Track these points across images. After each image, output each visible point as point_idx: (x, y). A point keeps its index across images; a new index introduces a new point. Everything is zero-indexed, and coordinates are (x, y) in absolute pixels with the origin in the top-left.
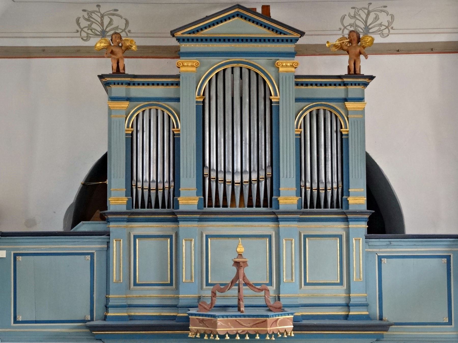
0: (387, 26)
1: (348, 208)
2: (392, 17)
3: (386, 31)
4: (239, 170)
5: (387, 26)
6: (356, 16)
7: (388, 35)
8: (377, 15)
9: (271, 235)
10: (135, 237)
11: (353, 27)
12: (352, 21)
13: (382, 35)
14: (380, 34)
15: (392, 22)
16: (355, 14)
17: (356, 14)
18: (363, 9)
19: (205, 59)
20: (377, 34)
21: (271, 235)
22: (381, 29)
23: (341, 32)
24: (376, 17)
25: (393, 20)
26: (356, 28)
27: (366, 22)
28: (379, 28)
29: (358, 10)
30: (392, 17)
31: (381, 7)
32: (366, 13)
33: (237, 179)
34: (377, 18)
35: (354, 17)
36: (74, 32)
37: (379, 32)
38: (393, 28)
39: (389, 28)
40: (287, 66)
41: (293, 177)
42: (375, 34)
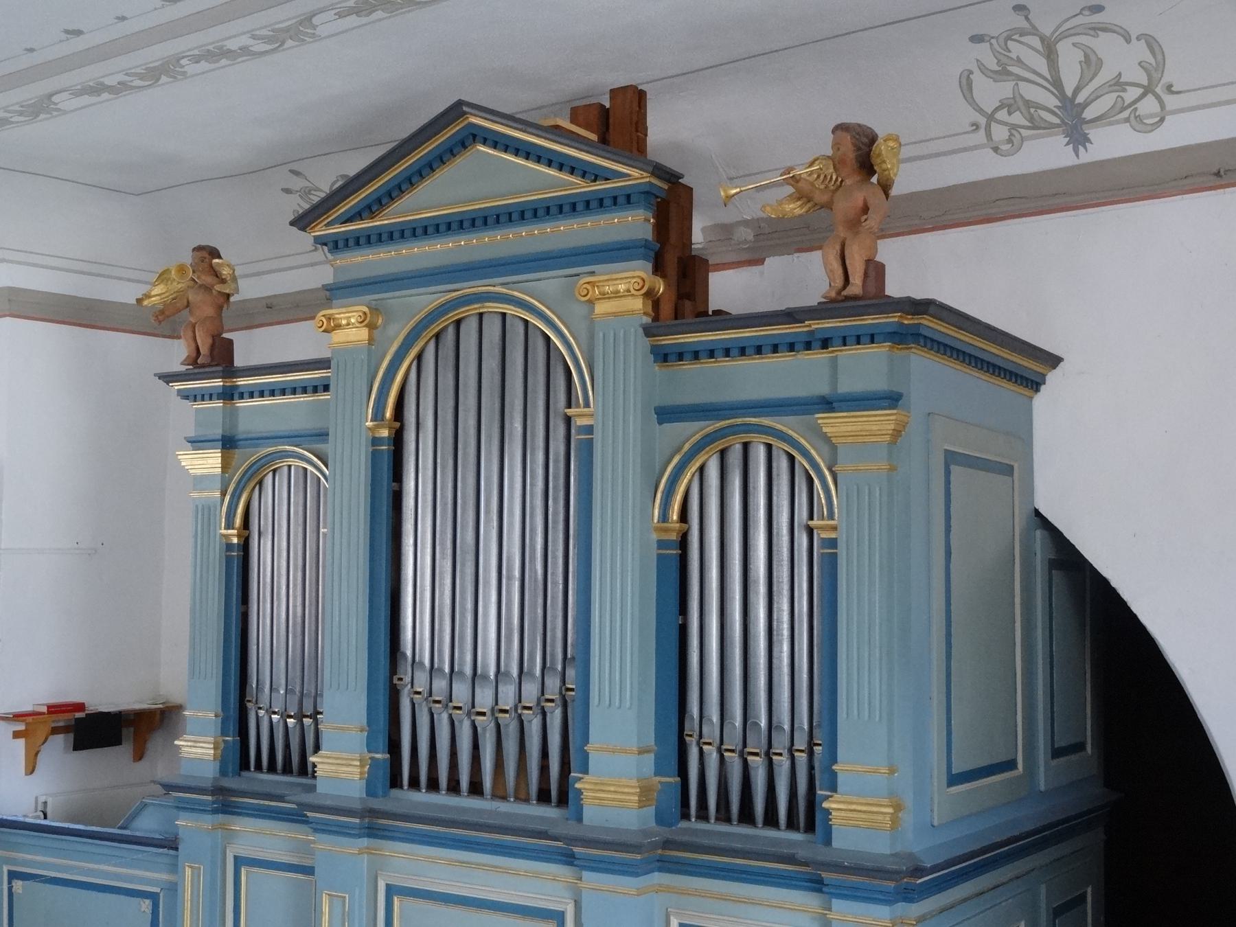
0: (1145, 83)
1: (828, 841)
2: (1151, 43)
3: (1149, 106)
4: (468, 670)
5: (1145, 83)
6: (1010, 68)
7: (1162, 120)
8: (1088, 51)
9: (563, 912)
10: (239, 861)
11: (1019, 109)
12: (1005, 89)
13: (1140, 124)
14: (1127, 120)
15: (1161, 66)
16: (999, 61)
17: (1004, 60)
18: (1016, 37)
19: (397, 299)
20: (1118, 122)
21: (563, 912)
22: (1126, 104)
23: (980, 136)
24: (1086, 56)
25: (1160, 57)
26: (1029, 112)
27: (1057, 83)
28: (1118, 96)
29: (1001, 40)
30: (1151, 43)
31: (1080, 13)
32: (1041, 49)
33: (484, 699)
34: (1091, 63)
35: (1002, 74)
36: (310, 251)
37: (1121, 112)
38: (1173, 89)
39: (1158, 90)
40: (616, 295)
41: (630, 708)
42: (1111, 124)
